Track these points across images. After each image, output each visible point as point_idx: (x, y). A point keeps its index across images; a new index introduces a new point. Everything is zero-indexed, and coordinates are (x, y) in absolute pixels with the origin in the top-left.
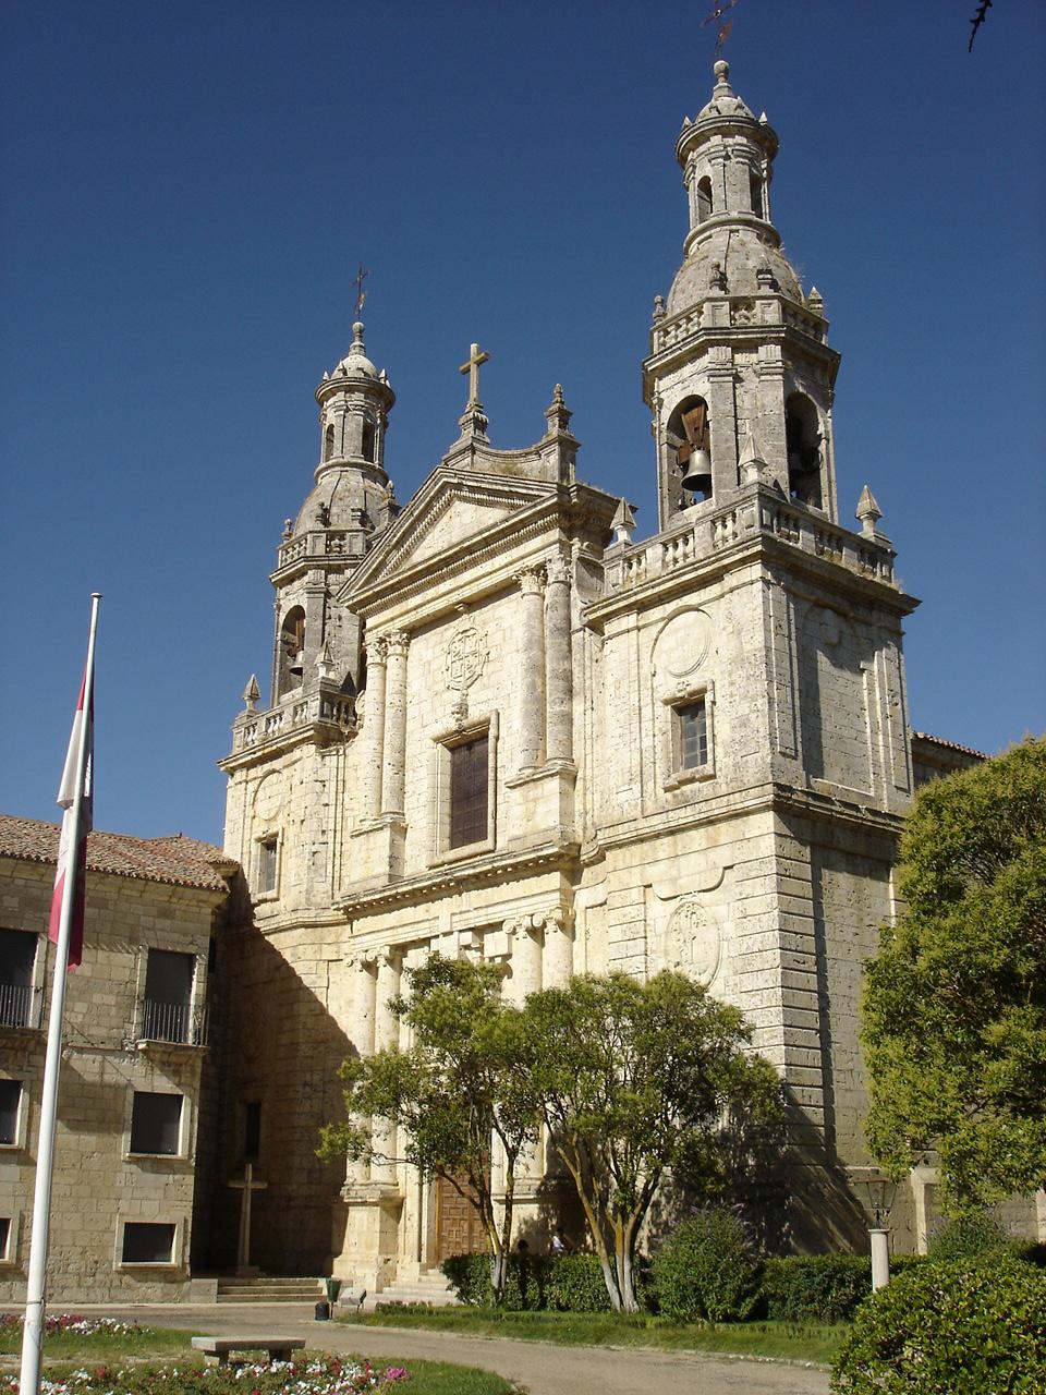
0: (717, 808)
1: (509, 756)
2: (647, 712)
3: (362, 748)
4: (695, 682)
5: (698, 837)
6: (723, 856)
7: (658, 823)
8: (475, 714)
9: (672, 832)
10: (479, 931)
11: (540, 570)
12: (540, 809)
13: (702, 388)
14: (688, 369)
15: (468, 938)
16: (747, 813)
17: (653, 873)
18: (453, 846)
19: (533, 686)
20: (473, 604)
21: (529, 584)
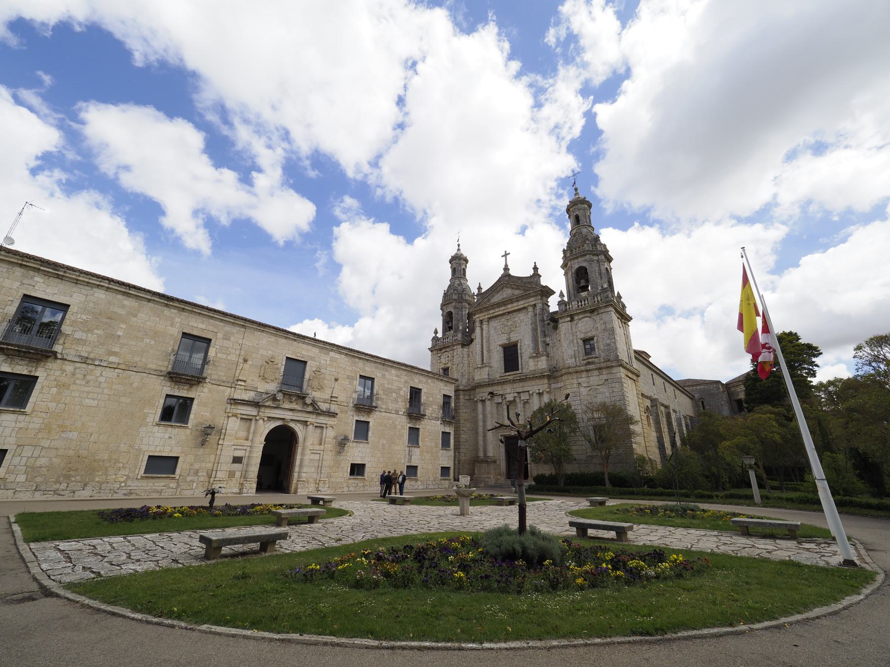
0: (602, 365)
1: (526, 349)
2: (575, 341)
3: (476, 346)
4: (590, 335)
5: (596, 373)
6: (604, 377)
7: (583, 368)
8: (513, 339)
9: (587, 371)
10: (519, 393)
11: (535, 305)
12: (540, 363)
13: (585, 264)
14: (580, 259)
15: (516, 395)
16: (612, 367)
17: (580, 380)
18: (506, 372)
19: (533, 334)
20: (509, 313)
21: (530, 309)
